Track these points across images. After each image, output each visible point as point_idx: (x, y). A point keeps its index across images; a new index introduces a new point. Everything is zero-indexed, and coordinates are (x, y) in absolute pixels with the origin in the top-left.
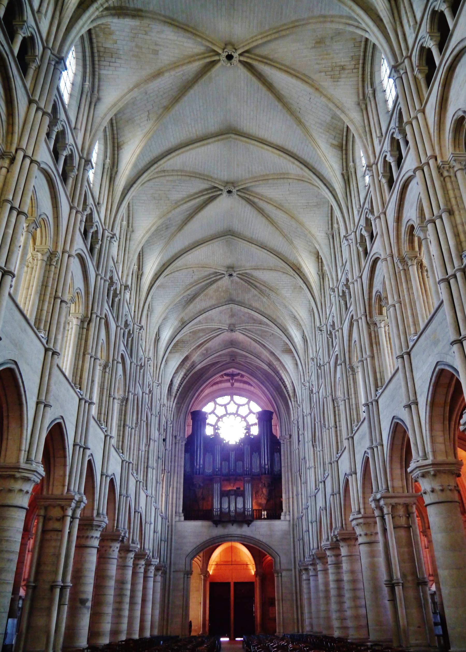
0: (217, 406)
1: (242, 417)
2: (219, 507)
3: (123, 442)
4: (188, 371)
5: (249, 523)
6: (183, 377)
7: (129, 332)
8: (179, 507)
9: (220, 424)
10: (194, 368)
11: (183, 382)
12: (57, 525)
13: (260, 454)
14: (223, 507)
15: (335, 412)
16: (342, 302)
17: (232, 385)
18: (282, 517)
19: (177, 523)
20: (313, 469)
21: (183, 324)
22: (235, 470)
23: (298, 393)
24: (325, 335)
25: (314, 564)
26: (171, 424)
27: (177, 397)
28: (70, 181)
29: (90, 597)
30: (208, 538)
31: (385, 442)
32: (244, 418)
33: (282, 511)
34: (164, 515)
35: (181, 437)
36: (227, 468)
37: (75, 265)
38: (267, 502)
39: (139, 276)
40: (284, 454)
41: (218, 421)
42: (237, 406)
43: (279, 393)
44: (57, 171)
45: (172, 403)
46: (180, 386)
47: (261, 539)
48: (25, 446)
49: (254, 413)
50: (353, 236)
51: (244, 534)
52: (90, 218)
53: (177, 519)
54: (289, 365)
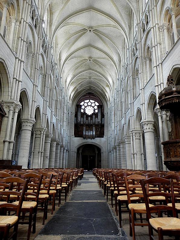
3: (56, 113)
5: (94, 138)
7: (57, 79)
9: (85, 109)
12: (39, 136)
15: (121, 106)
16: (126, 71)
17: (90, 96)
18: (104, 137)
21: (74, 76)
24: (120, 81)
25: (113, 150)
28: (37, 28)
29: (49, 156)
31: (135, 115)
32: (93, 107)
34: (68, 135)
37: (40, 57)
39: (60, 60)
41: (85, 108)
44: (34, 25)
46: (73, 96)
48: (30, 114)
50: (130, 49)
52: (44, 41)
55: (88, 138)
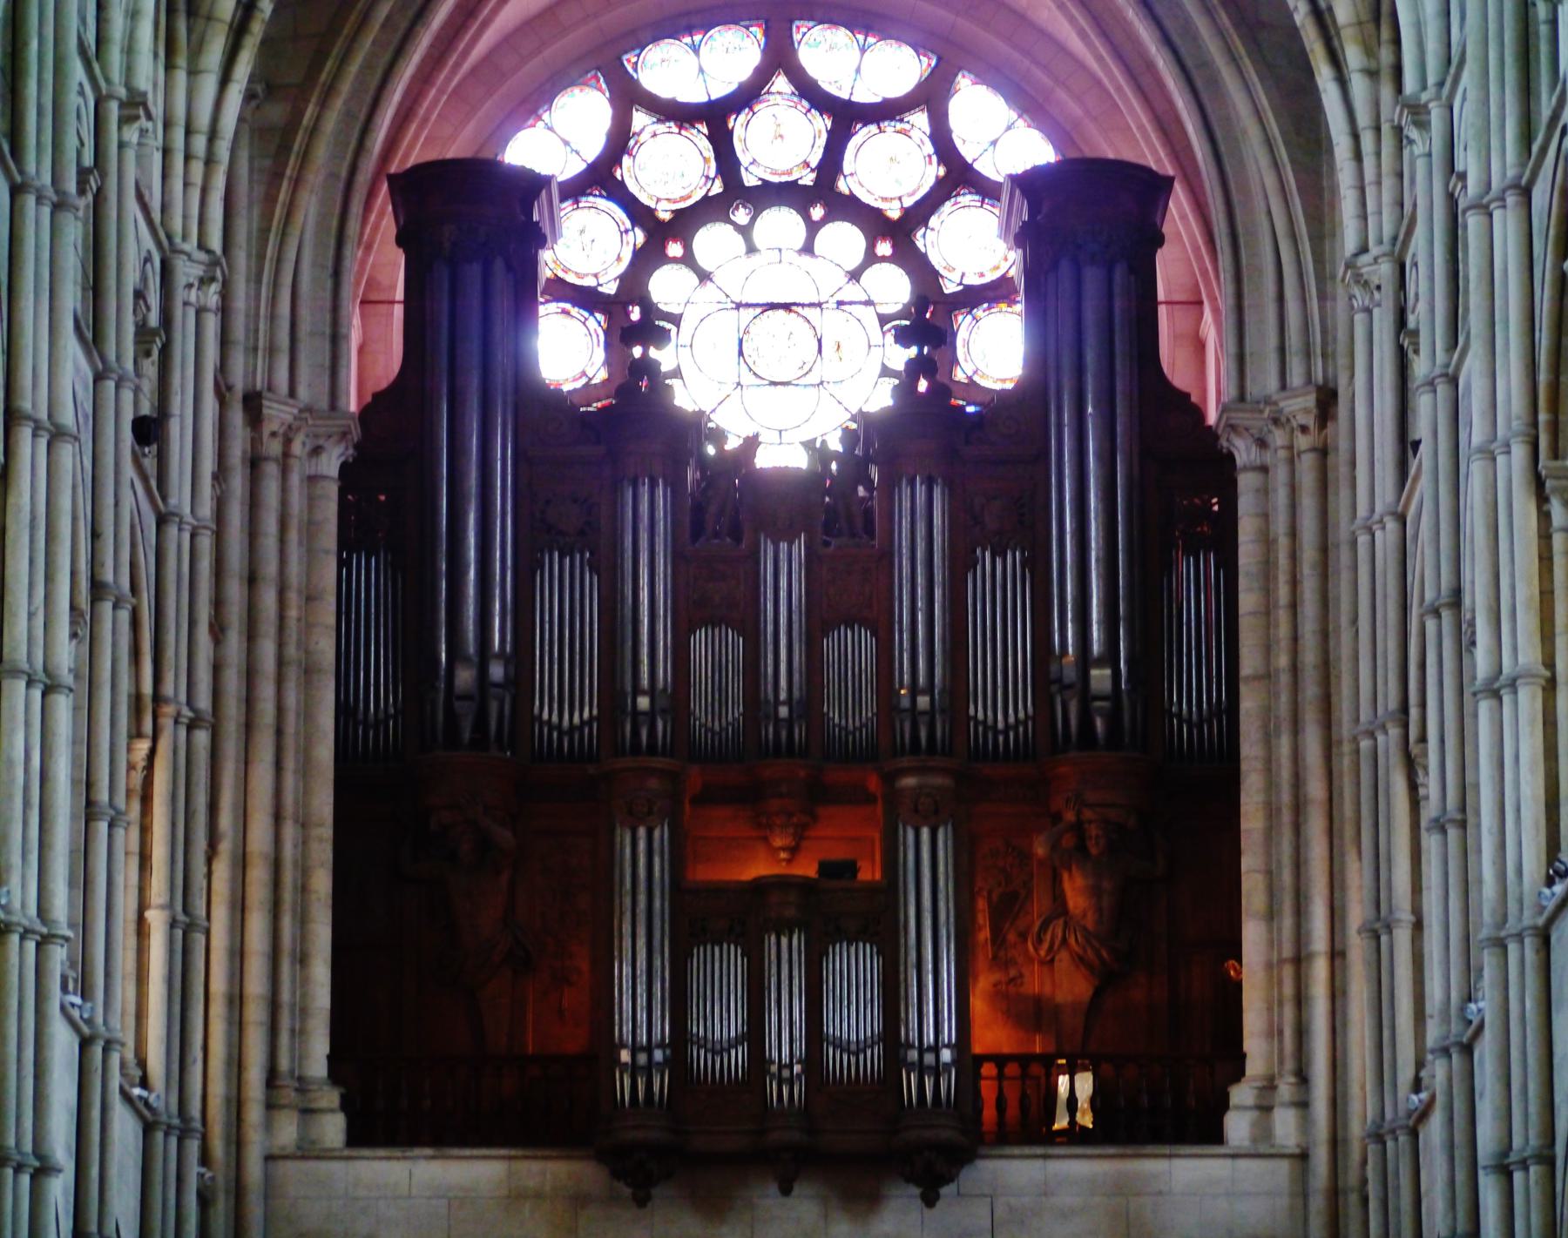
0: (640, 119)
1: (872, 221)
2: (663, 1028)
8: (300, 1033)
14: (697, 1029)
18: (1238, 1126)
19: (290, 1171)
20: (1529, 700)
22: (809, 704)
26: (205, 281)
27: (257, 29)
33: (1238, 1074)
34: (160, 1094)
35: (309, 409)
36: (736, 687)
38: (1097, 993)
41: (647, 259)
45: (209, 85)
49: (986, 190)
53: (288, 1131)
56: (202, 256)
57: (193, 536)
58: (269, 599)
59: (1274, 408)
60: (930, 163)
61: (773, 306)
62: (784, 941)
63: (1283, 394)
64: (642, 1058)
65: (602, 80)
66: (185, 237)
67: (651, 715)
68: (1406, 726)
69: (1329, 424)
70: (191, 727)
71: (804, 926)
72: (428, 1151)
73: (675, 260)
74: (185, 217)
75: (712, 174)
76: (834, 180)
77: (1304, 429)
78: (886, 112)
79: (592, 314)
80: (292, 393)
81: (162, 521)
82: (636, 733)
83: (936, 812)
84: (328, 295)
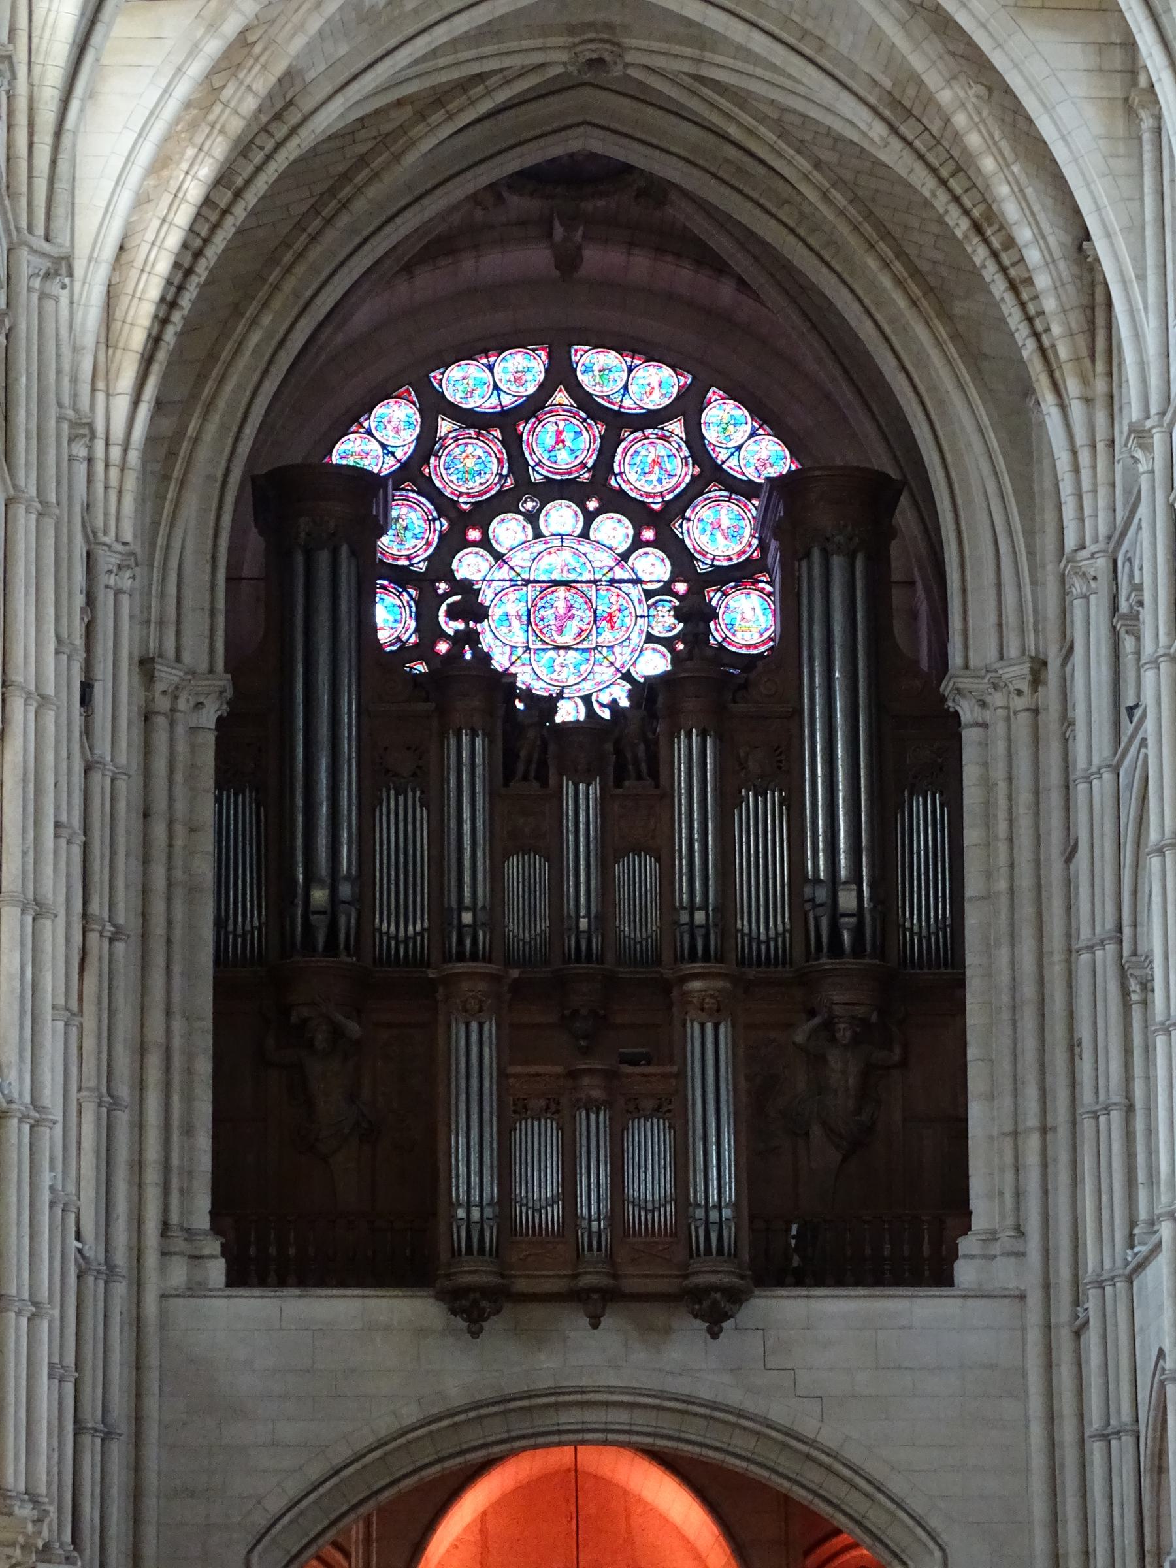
2: (491, 1190)
4: (243, 149)
6: (207, 202)
10: (294, 131)
11: (206, 241)
13: (793, 805)
14: (520, 1191)
17: (568, 262)
18: (965, 1272)
22: (602, 920)
23: (1138, 336)
27: (162, 355)
30: (410, 1414)
33: (966, 1229)
36: (543, 906)
38: (845, 1159)
40: (988, 805)
41: (451, 544)
42: (598, 429)
43: (956, 336)
47: (808, 1427)
49: (741, 489)
51: (682, 1385)
53: (179, 1274)
54: (1064, 111)
55: (577, 1297)
56: (119, 547)
57: (113, 780)
58: (159, 830)
59: (994, 675)
60: (687, 465)
61: (556, 583)
62: (593, 1117)
63: (1001, 664)
64: (476, 1214)
65: (413, 394)
66: (105, 533)
67: (474, 926)
68: (1120, 942)
69: (1040, 689)
70: (111, 940)
71: (609, 1104)
72: (297, 1291)
73: (474, 544)
74: (106, 514)
75: (505, 472)
76: (607, 479)
77: (1019, 693)
78: (651, 420)
79: (405, 590)
80: (178, 659)
81: (88, 769)
82: (461, 942)
83: (718, 1011)
84: (207, 577)
